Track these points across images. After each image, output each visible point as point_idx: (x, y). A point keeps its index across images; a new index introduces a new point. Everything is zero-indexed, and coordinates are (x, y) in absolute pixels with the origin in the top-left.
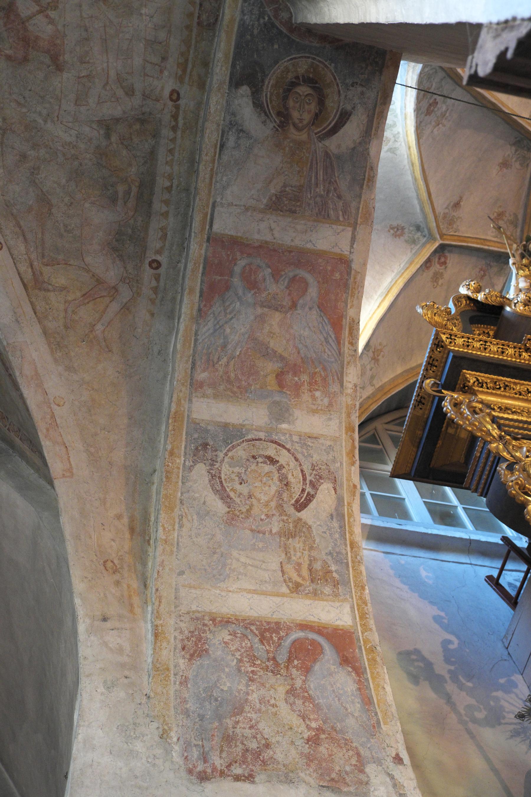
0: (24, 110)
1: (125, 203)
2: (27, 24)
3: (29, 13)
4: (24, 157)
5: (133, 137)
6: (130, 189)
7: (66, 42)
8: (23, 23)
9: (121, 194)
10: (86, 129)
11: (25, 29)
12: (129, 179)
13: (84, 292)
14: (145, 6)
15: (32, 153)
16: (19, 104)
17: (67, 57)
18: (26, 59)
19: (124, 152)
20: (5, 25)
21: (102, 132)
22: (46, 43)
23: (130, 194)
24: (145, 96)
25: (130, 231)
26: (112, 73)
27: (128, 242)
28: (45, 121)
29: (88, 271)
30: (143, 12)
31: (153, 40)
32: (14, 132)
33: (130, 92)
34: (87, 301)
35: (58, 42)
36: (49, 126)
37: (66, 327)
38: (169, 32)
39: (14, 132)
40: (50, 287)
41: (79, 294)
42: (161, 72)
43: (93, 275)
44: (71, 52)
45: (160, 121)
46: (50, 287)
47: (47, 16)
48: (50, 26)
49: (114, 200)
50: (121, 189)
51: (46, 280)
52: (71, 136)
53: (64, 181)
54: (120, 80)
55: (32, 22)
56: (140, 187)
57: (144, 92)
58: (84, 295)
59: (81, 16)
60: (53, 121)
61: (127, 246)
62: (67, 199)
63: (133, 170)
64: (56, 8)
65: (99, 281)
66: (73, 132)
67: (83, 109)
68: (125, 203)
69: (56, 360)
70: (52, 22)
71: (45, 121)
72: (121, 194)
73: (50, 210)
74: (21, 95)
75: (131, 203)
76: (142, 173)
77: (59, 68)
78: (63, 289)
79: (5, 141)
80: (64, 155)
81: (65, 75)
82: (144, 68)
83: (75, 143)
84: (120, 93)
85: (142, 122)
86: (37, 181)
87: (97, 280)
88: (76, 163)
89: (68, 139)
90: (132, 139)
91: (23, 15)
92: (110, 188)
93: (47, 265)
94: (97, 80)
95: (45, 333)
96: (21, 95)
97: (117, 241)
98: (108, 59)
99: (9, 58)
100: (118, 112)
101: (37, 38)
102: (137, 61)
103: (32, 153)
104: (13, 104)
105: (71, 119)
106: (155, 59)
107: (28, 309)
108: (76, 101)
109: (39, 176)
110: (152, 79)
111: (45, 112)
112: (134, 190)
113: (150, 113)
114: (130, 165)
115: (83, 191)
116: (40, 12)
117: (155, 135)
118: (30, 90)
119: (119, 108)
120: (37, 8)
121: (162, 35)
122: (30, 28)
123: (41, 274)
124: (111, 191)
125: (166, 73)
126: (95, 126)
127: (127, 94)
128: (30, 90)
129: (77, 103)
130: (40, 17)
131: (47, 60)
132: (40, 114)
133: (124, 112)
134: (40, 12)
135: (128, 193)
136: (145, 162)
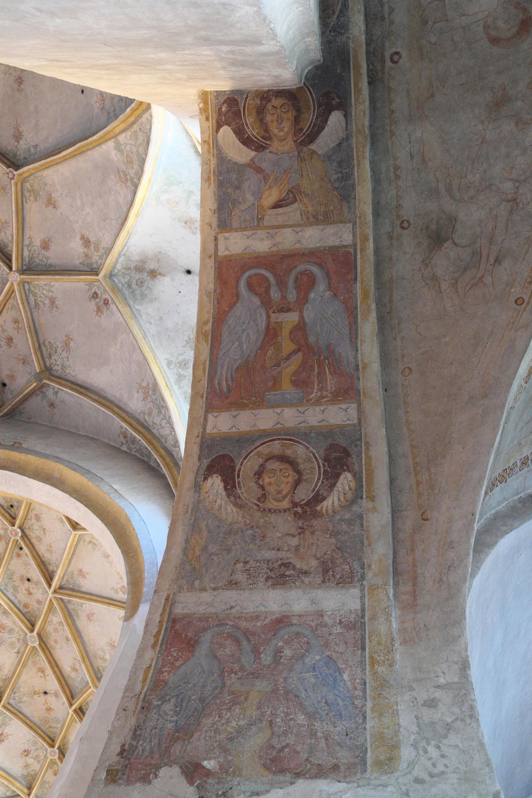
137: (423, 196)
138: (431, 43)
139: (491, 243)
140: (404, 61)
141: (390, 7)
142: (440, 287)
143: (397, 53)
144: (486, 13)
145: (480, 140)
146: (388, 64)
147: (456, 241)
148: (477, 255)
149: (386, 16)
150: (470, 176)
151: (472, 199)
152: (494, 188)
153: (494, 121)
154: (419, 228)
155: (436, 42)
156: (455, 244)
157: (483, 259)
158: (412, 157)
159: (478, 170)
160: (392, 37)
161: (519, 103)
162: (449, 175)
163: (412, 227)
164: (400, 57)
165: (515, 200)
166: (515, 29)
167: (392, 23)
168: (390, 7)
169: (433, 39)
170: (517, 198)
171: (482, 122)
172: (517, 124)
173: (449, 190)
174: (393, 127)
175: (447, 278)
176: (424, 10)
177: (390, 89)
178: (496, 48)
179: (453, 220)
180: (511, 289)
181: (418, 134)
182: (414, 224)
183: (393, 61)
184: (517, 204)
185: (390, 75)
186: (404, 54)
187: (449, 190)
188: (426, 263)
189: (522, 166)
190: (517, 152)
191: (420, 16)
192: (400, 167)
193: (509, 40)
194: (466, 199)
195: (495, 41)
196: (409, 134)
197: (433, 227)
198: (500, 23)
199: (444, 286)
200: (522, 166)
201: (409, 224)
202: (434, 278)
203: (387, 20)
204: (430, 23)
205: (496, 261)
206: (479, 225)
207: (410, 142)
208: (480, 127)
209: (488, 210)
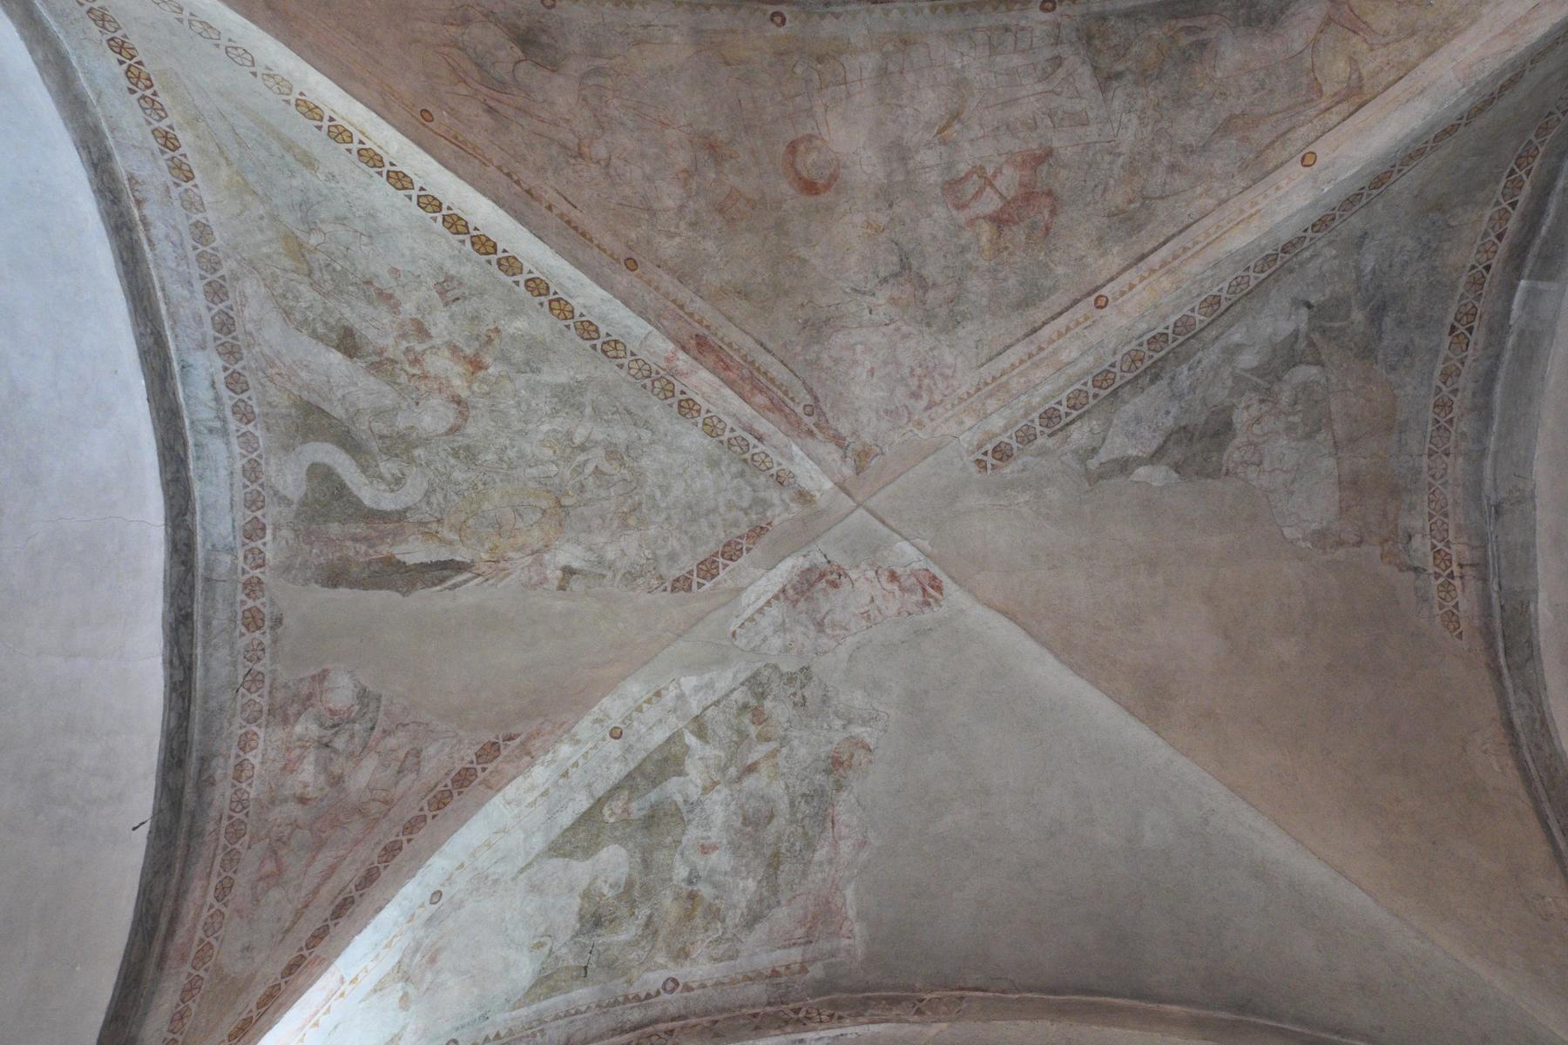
0: (1112, 182)
1: (1202, 29)
2: (1009, 198)
3: (996, 197)
4: (1173, 168)
5: (1112, 45)
6: (1182, 29)
7: (1017, 150)
8: (1009, 203)
9: (1192, 39)
10: (1116, 104)
11: (1015, 199)
12: (1171, 33)
13: (1351, 34)
14: (953, 64)
15: (1165, 160)
16: (1105, 190)
17: (1034, 146)
18: (1049, 193)
19: (1134, 49)
20: (1016, 223)
21: (1115, 84)
22: (1024, 173)
23: (1189, 27)
24: (1058, 41)
25: (1242, 11)
26: (1039, 88)
27: (1258, 8)
28: (1120, 155)
29: (1316, 40)
30: (959, 66)
31: (987, 47)
32: (1143, 188)
33: (1057, 61)
34: (1363, 26)
35: (1019, 159)
36: (1124, 149)
37: (1413, 34)
38: (974, 29)
39: (1143, 188)
40: (1354, 77)
41: (1355, 39)
42: (1023, 29)
43: (1322, 31)
44: (1027, 142)
45: (1083, 16)
46: (1354, 77)
47: (995, 176)
48: (1004, 171)
49: (1202, 45)
50: (1185, 41)
51: (1345, 85)
52: (1129, 120)
53: (1193, 112)
54: (1045, 77)
55: (1004, 192)
56: (1176, 18)
57: (1052, 45)
58: (1354, 32)
59: (983, 137)
60: (1117, 146)
61: (1265, 7)
62: (1217, 101)
63: (1155, 32)
64: (982, 168)
65: (1329, 21)
66: (1125, 118)
67: (1091, 115)
68: (1202, 29)
69: (1474, 21)
70: (998, 171)
71: (1120, 155)
72: (1192, 39)
73: (1237, 116)
74: (1093, 190)
75: (1201, 22)
76: (1158, 19)
77: (1049, 153)
78: (1352, 60)
79: (1158, 195)
80: (1157, 121)
81: (1056, 144)
82: (1023, 51)
83: (1138, 113)
84: (1061, 73)
85: (1090, 38)
86: (1201, 144)
87: (1327, 24)
88: (1165, 104)
89: (1135, 121)
90: (1115, 46)
91: (1001, 205)
92: (1187, 54)
93: (1321, 91)
94: (1053, 105)
95: (1429, 54)
96: (1093, 190)
97: (1260, 22)
98: (1024, 97)
99: (1053, 213)
100: (1085, 71)
101: (1021, 185)
102: (1017, 60)
103: (1165, 160)
104: (1109, 196)
105: (1109, 126)
106: (1010, 39)
107: (1398, 88)
108: (1083, 125)
109: (1194, 143)
110: (1035, 39)
111: (1108, 158)
112: (1182, 23)
113: (1078, 30)
114: (1150, 37)
115: (1201, 85)
116: (992, 185)
117: (1103, 17)
118: (1085, 181)
119: (1080, 70)
120: (988, 189)
121: (980, 37)
122: (1012, 193)
123: (1335, 94)
124: (1191, 51)
125: (1023, 23)
126: (1110, 95)
127: (1060, 65)
128: (1085, 181)
129: (1085, 124)
130: (997, 183)
131: (1045, 167)
132: (1111, 163)
133: (1084, 62)
134: (992, 185)
135: (1189, 30)
136: (1142, 20)
137: (589, 35)
138: (794, 66)
139: (516, 108)
140: (772, 30)
141: (841, 14)
142: (452, 24)
143: (783, 21)
144: (827, 138)
145: (666, 121)
146: (771, 9)
147: (523, 64)
148: (501, 86)
149: (829, 9)
150: (616, 102)
151: (584, 100)
152: (599, 132)
153: (691, 141)
154: (543, 20)
155: (794, 73)
156: (520, 61)
157: (496, 95)
158: (645, 27)
159: (624, 114)
160: (803, 15)
161: (713, 176)
162: (619, 75)
163: (545, 10)
164: (779, 26)
165: (581, 155)
166: (804, 174)
167: (822, 17)
168: (841, 14)
169: (799, 70)
170: (584, 159)
171: (690, 125)
172: (685, 171)
173: (597, 71)
174: (686, 6)
175: (466, 37)
176: (834, 58)
177: (738, 8)
178: (784, 149)
179: (555, 67)
180: (448, 113)
181: (676, 38)
182: (549, 14)
183: (774, 14)
184: (575, 158)
185: (756, 10)
186: (782, 30)
187: (597, 71)
188: (489, 15)
189: (628, 174)
190: (648, 169)
191: (827, 54)
192: (631, 8)
193: (792, 165)
194: (583, 92)
195: (793, 148)
196: (675, 26)
197: (544, 39)
198: (814, 156)
199: (453, 29)
200: (628, 174)
201: (549, 8)
202: (466, 21)
203: (826, 10)
204: (819, 66)
205: (491, 108)
206: (544, 101)
207: (666, 26)
208: (683, 121)
209: (567, 117)
